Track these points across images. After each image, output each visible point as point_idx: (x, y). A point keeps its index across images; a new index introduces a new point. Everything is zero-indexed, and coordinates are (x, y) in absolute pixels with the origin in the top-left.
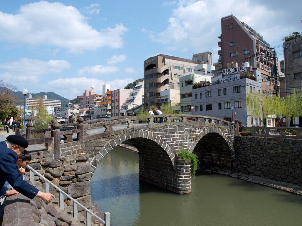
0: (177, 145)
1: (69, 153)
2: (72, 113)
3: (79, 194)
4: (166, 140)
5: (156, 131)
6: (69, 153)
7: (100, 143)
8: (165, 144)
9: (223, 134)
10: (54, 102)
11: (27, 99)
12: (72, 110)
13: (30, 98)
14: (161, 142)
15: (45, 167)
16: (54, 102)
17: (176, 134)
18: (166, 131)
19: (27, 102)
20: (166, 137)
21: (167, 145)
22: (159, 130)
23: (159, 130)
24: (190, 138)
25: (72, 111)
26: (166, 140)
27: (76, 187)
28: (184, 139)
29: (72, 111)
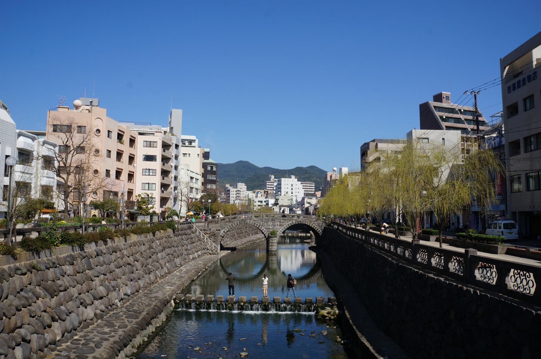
0: (270, 228)
1: (213, 227)
2: (309, 203)
3: (215, 241)
4: (262, 226)
5: (255, 221)
6: (213, 227)
7: (227, 225)
8: (261, 227)
9: (312, 225)
10: (308, 185)
11: (268, 182)
12: (309, 199)
13: (272, 180)
14: (259, 226)
15: (204, 230)
16: (308, 185)
17: (269, 223)
18: (262, 221)
19: (267, 186)
20: (262, 224)
21: (263, 228)
22: (258, 221)
23: (258, 221)
24: (279, 226)
25: (309, 201)
26: (262, 226)
27: (214, 238)
28: (275, 226)
29: (309, 201)
